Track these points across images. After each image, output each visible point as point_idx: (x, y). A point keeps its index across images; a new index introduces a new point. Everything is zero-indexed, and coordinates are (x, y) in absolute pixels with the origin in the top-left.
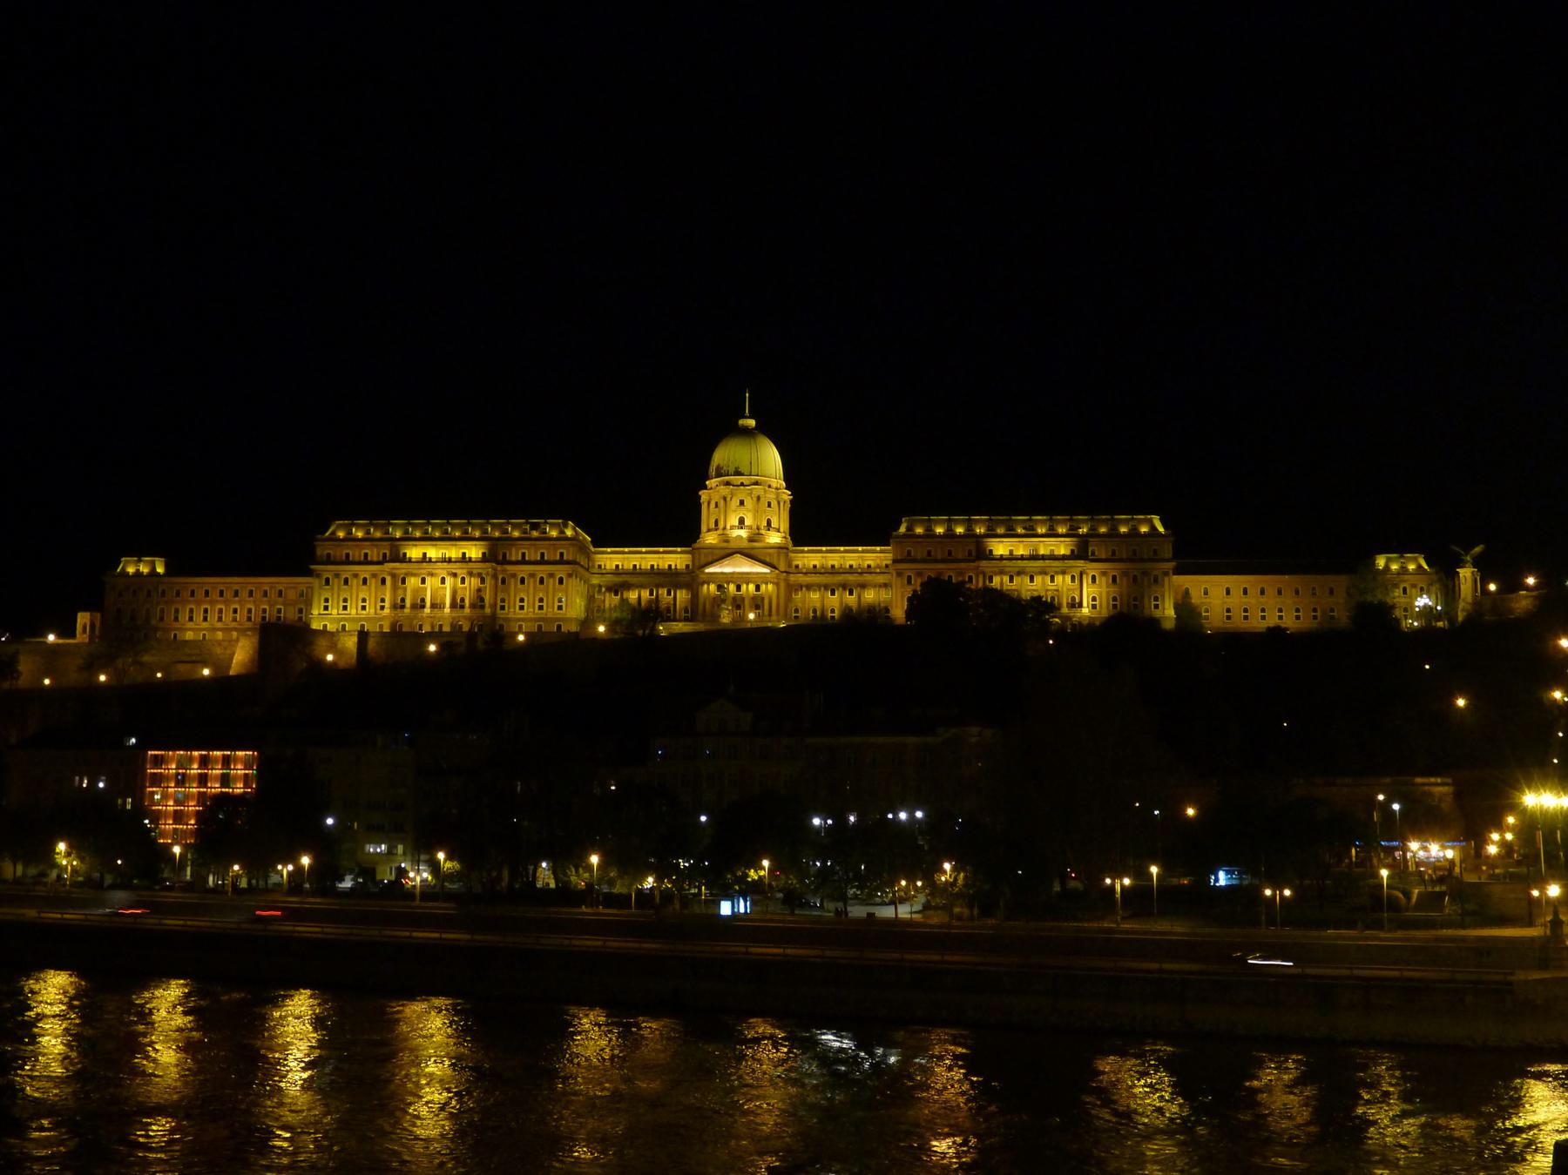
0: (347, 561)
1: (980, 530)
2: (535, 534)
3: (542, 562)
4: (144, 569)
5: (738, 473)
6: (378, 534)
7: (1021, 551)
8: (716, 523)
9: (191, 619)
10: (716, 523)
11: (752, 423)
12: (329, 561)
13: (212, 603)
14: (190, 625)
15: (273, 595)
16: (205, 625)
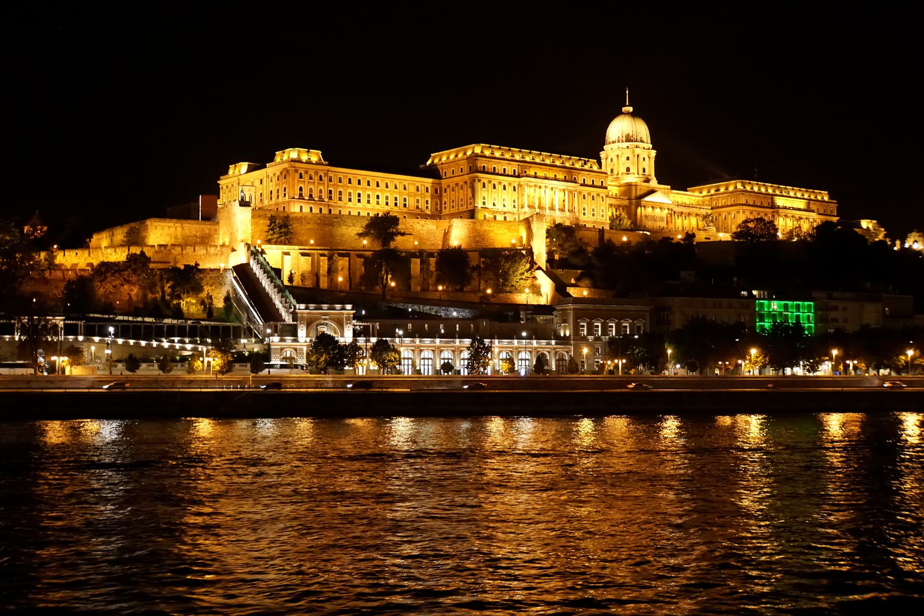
0: (494, 173)
1: (770, 191)
2: (586, 167)
3: (593, 186)
4: (314, 159)
5: (642, 141)
6: (507, 156)
7: (788, 205)
8: (628, 169)
9: (350, 200)
10: (628, 169)
11: (631, 109)
12: (484, 171)
13: (364, 189)
14: (350, 204)
15: (400, 188)
16: (359, 205)
